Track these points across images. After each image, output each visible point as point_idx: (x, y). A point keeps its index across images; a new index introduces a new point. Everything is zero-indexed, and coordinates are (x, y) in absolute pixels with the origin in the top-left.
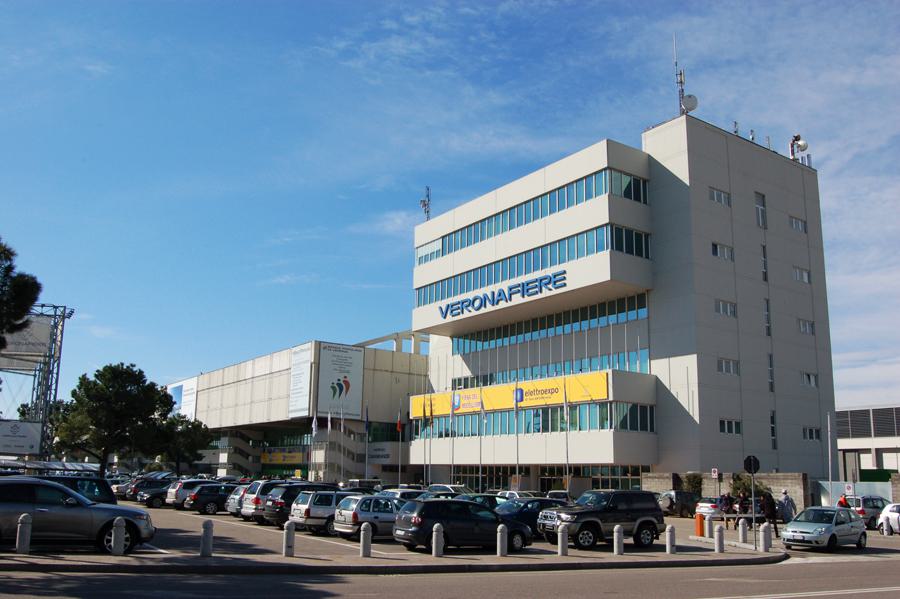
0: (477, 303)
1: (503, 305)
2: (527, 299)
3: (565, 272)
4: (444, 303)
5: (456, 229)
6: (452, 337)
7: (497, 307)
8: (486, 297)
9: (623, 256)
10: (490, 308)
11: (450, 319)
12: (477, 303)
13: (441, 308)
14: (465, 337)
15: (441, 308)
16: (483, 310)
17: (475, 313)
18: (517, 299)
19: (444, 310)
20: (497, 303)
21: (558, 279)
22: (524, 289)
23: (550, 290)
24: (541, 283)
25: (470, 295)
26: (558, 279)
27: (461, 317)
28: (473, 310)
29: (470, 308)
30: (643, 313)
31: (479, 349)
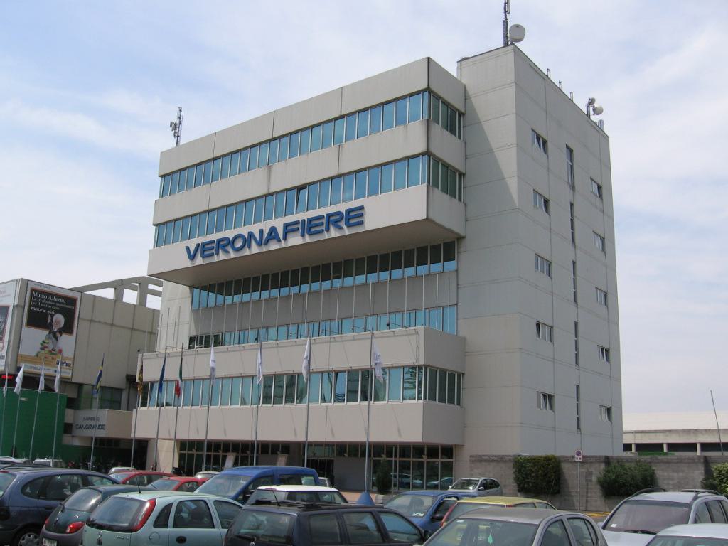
0: (239, 244)
1: (274, 246)
2: (308, 239)
3: (362, 208)
4: (192, 244)
5: (217, 155)
6: (192, 287)
7: (264, 249)
8: (251, 235)
9: (437, 193)
10: (255, 249)
11: (199, 261)
12: (239, 244)
13: (188, 248)
14: (210, 288)
15: (188, 248)
16: (246, 252)
17: (233, 255)
18: (295, 240)
19: (192, 251)
20: (267, 243)
21: (354, 216)
22: (309, 227)
23: (341, 228)
24: (333, 220)
25: (230, 234)
26: (354, 216)
27: (216, 259)
28: (231, 251)
29: (342, 224)
30: (450, 265)
31: (212, 304)
